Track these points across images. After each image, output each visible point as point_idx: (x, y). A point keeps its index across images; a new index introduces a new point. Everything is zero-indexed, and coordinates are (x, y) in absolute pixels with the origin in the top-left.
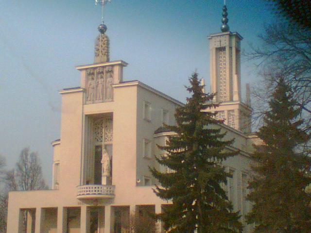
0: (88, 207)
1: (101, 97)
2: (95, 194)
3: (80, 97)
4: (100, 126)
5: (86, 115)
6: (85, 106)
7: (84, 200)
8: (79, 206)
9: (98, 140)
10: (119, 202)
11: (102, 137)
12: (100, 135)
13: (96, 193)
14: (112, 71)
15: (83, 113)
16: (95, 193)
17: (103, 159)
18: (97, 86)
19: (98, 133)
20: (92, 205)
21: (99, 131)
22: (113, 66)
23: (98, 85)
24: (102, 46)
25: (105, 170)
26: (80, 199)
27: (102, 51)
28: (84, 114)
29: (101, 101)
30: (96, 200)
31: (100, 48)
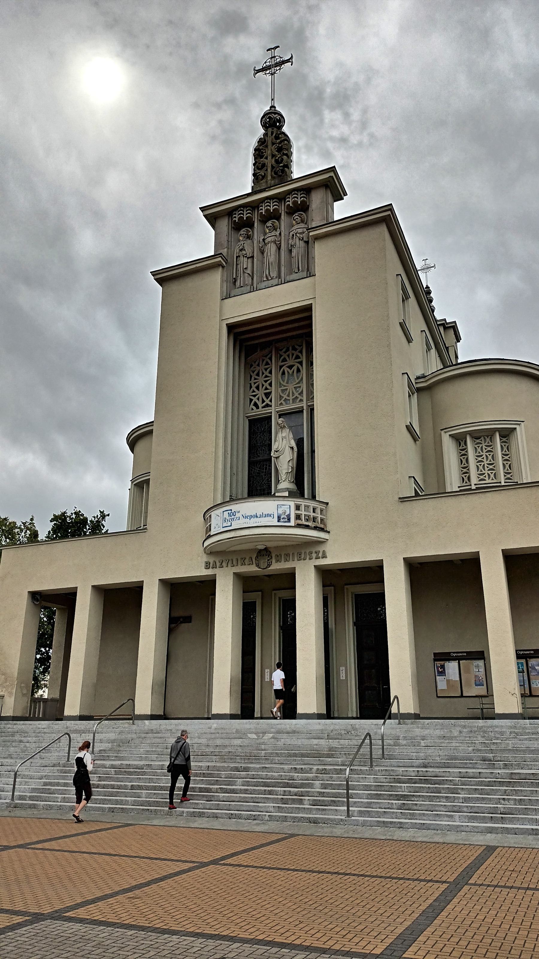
0: (236, 575)
1: (274, 274)
4: (262, 367)
8: (210, 572)
9: (256, 405)
11: (268, 395)
12: (261, 393)
14: (304, 208)
17: (274, 447)
19: (257, 388)
20: (251, 569)
21: (261, 379)
24: (273, 156)
25: (283, 476)
26: (211, 552)
27: (273, 167)
29: (275, 281)
30: (264, 552)
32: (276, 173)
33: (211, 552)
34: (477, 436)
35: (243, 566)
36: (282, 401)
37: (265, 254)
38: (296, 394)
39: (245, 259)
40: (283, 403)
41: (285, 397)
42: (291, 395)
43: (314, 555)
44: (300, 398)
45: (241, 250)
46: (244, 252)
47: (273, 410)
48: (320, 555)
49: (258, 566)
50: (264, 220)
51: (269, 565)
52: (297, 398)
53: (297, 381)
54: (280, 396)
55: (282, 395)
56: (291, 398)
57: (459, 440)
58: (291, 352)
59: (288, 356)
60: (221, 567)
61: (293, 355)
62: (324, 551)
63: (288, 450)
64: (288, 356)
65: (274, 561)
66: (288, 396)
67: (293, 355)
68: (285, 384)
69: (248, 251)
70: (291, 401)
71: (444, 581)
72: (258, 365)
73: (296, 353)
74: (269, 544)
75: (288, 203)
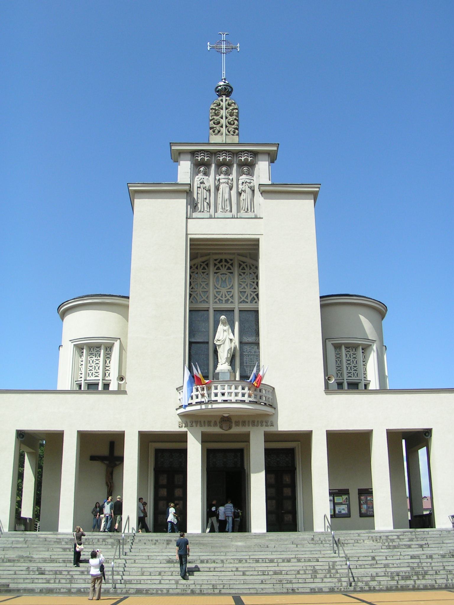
2: (243, 402)
3: (181, 203)
5: (191, 240)
6: (189, 220)
7: (190, 419)
8: (184, 429)
10: (287, 422)
13: (246, 398)
15: (187, 234)
16: (243, 399)
18: (217, 188)
22: (255, 154)
23: (219, 185)
24: (226, 118)
27: (226, 127)
28: (189, 236)
30: (226, 419)
31: (223, 121)
32: (229, 132)
33: (183, 416)
34: (348, 347)
35: (209, 427)
36: (216, 300)
37: (220, 191)
38: (228, 297)
39: (205, 191)
40: (218, 302)
41: (219, 297)
42: (224, 296)
43: (264, 424)
44: (231, 300)
45: (201, 183)
46: (204, 185)
47: (212, 306)
48: (269, 424)
49: (221, 427)
50: (219, 165)
51: (230, 428)
52: (228, 300)
53: (229, 287)
54: (215, 296)
55: (217, 295)
56: (224, 299)
57: (338, 347)
58: (224, 263)
59: (222, 266)
60: (192, 426)
61: (225, 266)
62: (271, 422)
63: (228, 341)
64: (222, 266)
65: (234, 425)
66: (222, 297)
67: (225, 266)
68: (218, 287)
69: (207, 185)
70: (224, 301)
71: (349, 447)
72: (197, 268)
73: (228, 265)
74: (232, 413)
75: (240, 158)
